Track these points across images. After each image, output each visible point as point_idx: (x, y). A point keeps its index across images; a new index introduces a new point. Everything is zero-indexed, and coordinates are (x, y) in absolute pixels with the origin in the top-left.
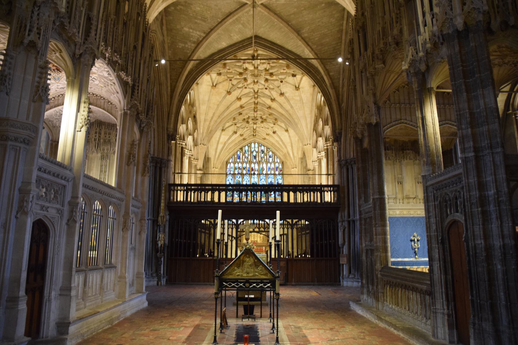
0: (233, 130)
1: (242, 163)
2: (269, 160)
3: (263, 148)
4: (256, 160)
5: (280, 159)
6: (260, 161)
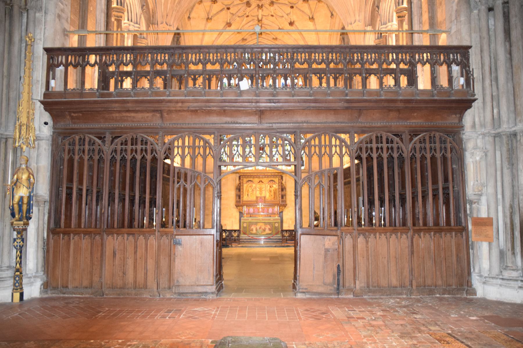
0: (226, 20)
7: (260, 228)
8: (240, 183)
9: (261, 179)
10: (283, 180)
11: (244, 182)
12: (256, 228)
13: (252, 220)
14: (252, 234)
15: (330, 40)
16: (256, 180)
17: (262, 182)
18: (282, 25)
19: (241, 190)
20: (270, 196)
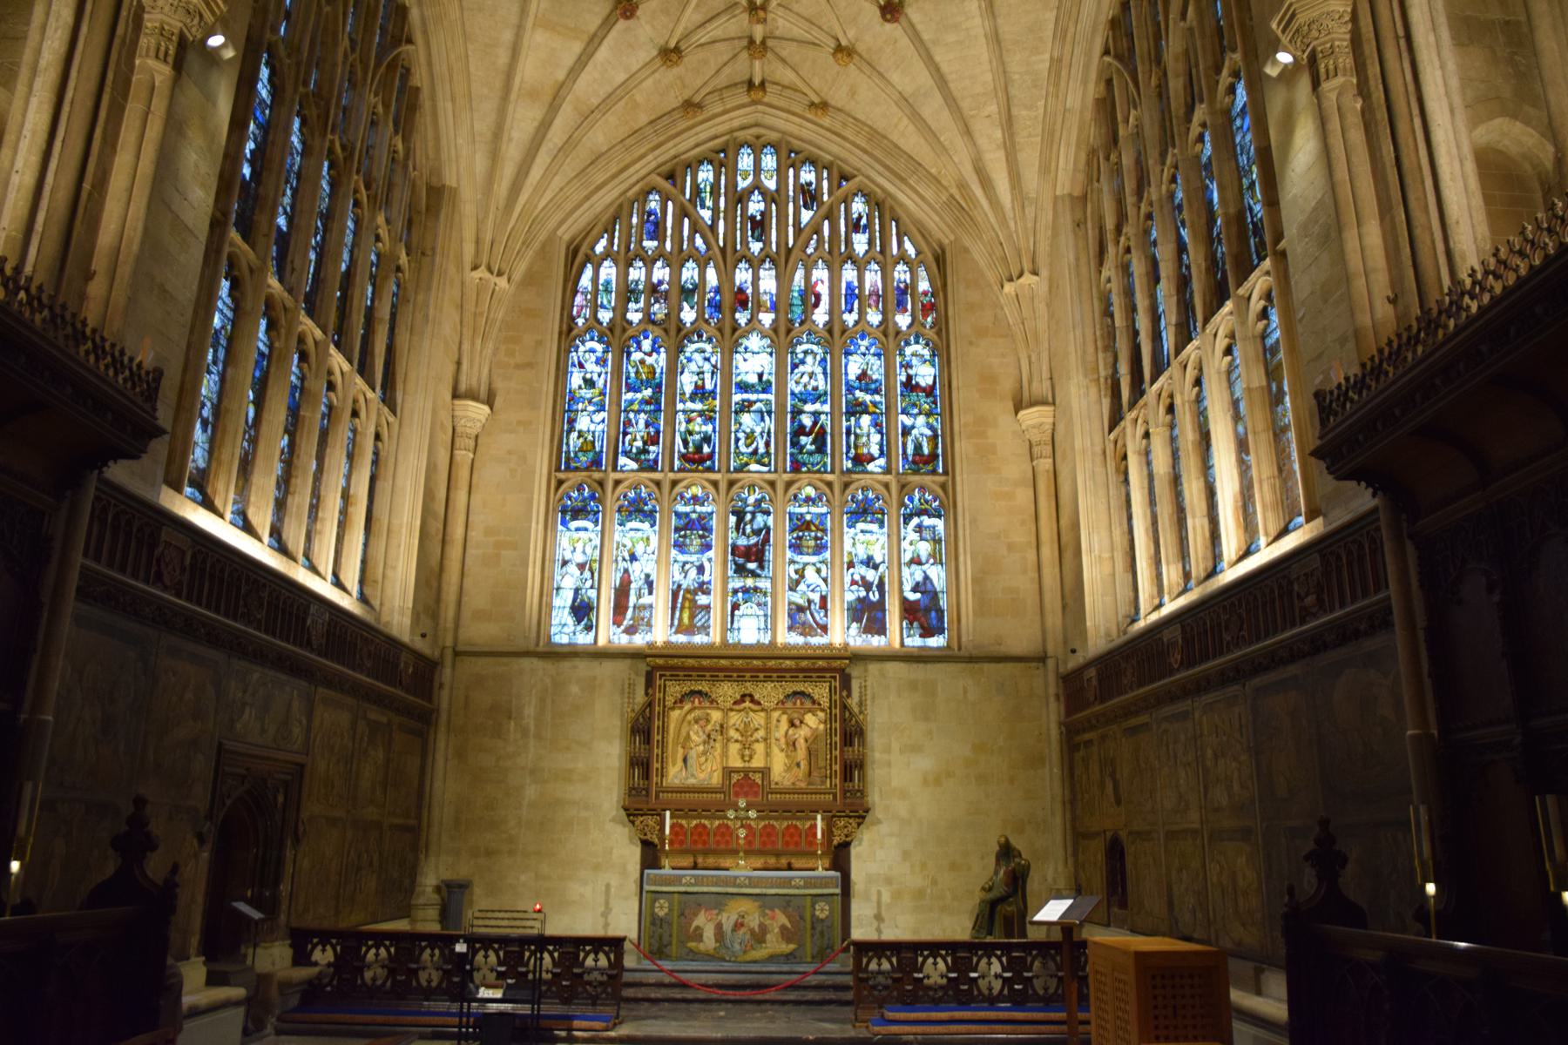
1: (676, 261)
2: (849, 242)
3: (808, 176)
4: (767, 243)
5: (922, 234)
6: (789, 251)
7: (738, 926)
8: (650, 705)
9: (749, 687)
10: (849, 695)
11: (670, 701)
12: (719, 927)
13: (699, 881)
14: (694, 955)
15: (1057, 85)
16: (727, 691)
17: (753, 701)
18: (851, 34)
19: (657, 737)
20: (788, 769)
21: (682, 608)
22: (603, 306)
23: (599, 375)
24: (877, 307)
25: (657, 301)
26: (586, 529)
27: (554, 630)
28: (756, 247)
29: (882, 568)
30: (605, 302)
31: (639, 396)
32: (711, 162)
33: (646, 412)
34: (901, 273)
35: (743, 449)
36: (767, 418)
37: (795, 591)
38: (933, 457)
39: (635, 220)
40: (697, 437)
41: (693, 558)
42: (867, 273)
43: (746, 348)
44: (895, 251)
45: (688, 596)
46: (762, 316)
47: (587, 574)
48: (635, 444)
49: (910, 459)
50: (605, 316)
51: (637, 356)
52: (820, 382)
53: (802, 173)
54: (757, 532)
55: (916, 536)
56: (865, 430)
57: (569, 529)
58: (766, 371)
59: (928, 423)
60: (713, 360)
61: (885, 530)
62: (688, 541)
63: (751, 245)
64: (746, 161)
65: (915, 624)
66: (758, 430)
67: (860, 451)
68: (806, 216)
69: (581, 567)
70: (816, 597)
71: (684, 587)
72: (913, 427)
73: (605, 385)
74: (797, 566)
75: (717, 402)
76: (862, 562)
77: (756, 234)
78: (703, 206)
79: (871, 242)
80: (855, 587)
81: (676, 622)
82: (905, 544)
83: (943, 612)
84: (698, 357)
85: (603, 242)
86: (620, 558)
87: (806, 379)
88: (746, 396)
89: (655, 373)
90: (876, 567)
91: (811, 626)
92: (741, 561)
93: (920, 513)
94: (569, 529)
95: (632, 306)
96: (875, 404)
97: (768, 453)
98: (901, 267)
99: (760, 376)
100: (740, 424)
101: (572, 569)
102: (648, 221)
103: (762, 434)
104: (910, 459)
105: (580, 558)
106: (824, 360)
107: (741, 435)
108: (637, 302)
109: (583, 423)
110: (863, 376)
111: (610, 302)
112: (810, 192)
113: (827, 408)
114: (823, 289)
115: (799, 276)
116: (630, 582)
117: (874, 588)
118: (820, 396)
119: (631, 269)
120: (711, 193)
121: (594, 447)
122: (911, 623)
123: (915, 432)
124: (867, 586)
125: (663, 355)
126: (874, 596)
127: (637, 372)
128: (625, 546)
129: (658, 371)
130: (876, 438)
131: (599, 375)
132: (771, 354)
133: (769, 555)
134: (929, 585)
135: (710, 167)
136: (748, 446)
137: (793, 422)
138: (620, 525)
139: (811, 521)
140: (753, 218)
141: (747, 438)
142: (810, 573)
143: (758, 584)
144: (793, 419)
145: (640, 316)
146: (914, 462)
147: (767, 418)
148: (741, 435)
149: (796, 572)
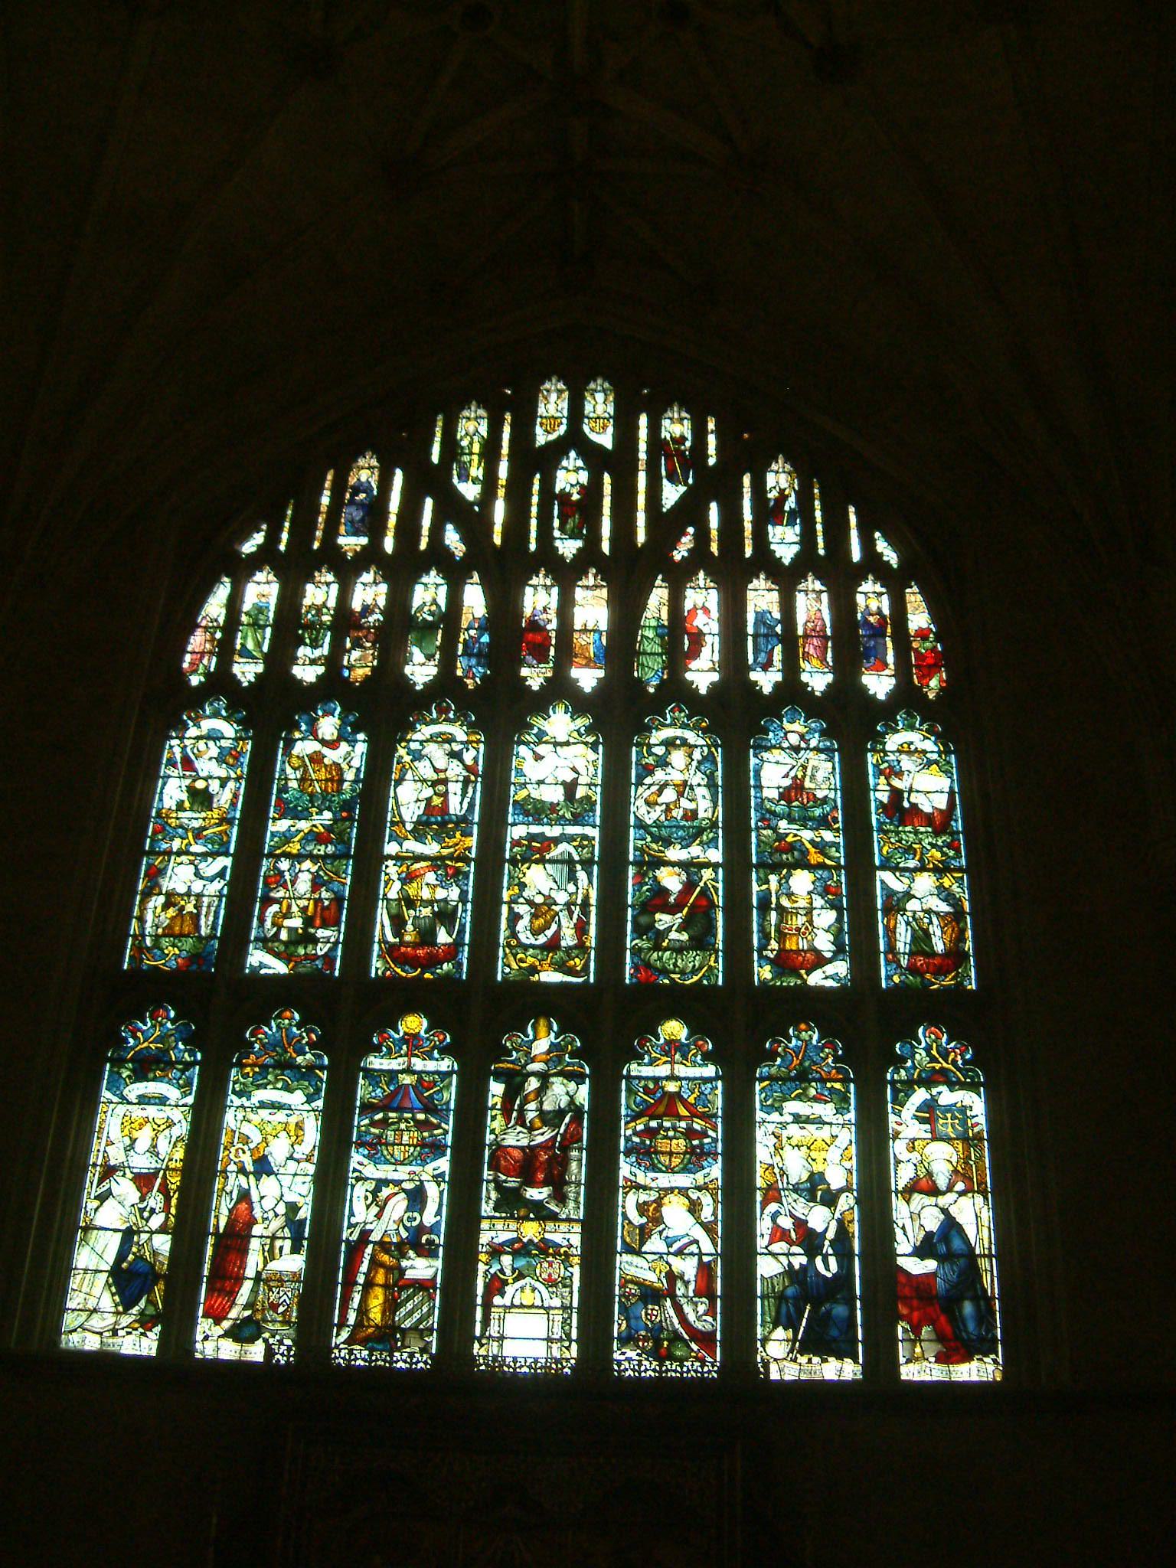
3: (676, 427)
4: (594, 539)
21: (369, 1285)
22: (245, 653)
23: (223, 785)
24: (823, 660)
25: (357, 644)
26: (162, 1101)
27: (70, 1320)
28: (568, 547)
29: (846, 1202)
30: (250, 645)
31: (304, 825)
32: (483, 403)
33: (314, 858)
34: (871, 598)
35: (525, 937)
36: (582, 875)
37: (639, 1253)
38: (955, 957)
39: (325, 500)
40: (426, 912)
41: (402, 1173)
42: (800, 598)
43: (541, 734)
44: (856, 555)
45: (385, 1258)
46: (575, 673)
47: (156, 1200)
48: (287, 923)
49: (904, 962)
50: (246, 671)
51: (304, 748)
52: (704, 805)
53: (666, 423)
54: (550, 1119)
55: (920, 1130)
56: (802, 903)
57: (124, 1100)
58: (583, 780)
59: (941, 888)
60: (468, 757)
61: (852, 1116)
62: (390, 1135)
63: (558, 543)
64: (553, 404)
65: (926, 1331)
66: (562, 898)
67: (790, 945)
68: (671, 494)
69: (144, 1181)
70: (688, 1267)
71: (375, 1237)
72: (909, 896)
73: (233, 804)
74: (644, 1197)
75: (473, 841)
76: (796, 1189)
77: (570, 525)
78: (464, 476)
79: (807, 538)
80: (780, 1247)
81: (352, 1317)
82: (898, 1148)
83: (989, 1301)
84: (437, 754)
85: (259, 538)
86: (232, 1167)
87: (669, 795)
88: (535, 829)
89: (341, 781)
90: (830, 1200)
91: (676, 1337)
92: (512, 1182)
93: (927, 1082)
94: (124, 1100)
95: (303, 652)
96: (821, 847)
97: (581, 947)
98: (869, 586)
99: (570, 788)
100: (523, 886)
101: (125, 1189)
102: (352, 502)
103: (568, 905)
104: (904, 962)
105: (142, 1162)
106: (709, 758)
107: (523, 909)
108: (315, 644)
109: (179, 877)
110: (794, 791)
111: (259, 645)
112: (680, 454)
113: (716, 855)
114: (708, 621)
115: (658, 598)
116: (253, 1221)
117: (827, 1248)
118: (700, 831)
119: (309, 587)
120: (481, 455)
121: (197, 927)
122: (916, 1329)
123: (912, 905)
124: (810, 1241)
125: (361, 748)
126: (828, 1267)
127: (302, 780)
128: (246, 1140)
129: (350, 775)
130: (826, 918)
131: (223, 785)
132: (594, 747)
133: (578, 1169)
134: (957, 1244)
135: (481, 412)
136: (536, 933)
137: (639, 884)
138: (239, 1094)
139: (678, 1095)
140: (564, 497)
141: (535, 916)
142: (675, 1214)
143: (557, 1238)
144: (640, 876)
145: (321, 670)
146: (912, 969)
147: (582, 875)
148: (523, 909)
149: (642, 1208)
